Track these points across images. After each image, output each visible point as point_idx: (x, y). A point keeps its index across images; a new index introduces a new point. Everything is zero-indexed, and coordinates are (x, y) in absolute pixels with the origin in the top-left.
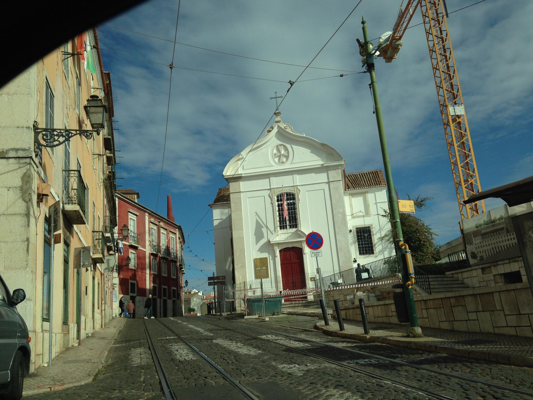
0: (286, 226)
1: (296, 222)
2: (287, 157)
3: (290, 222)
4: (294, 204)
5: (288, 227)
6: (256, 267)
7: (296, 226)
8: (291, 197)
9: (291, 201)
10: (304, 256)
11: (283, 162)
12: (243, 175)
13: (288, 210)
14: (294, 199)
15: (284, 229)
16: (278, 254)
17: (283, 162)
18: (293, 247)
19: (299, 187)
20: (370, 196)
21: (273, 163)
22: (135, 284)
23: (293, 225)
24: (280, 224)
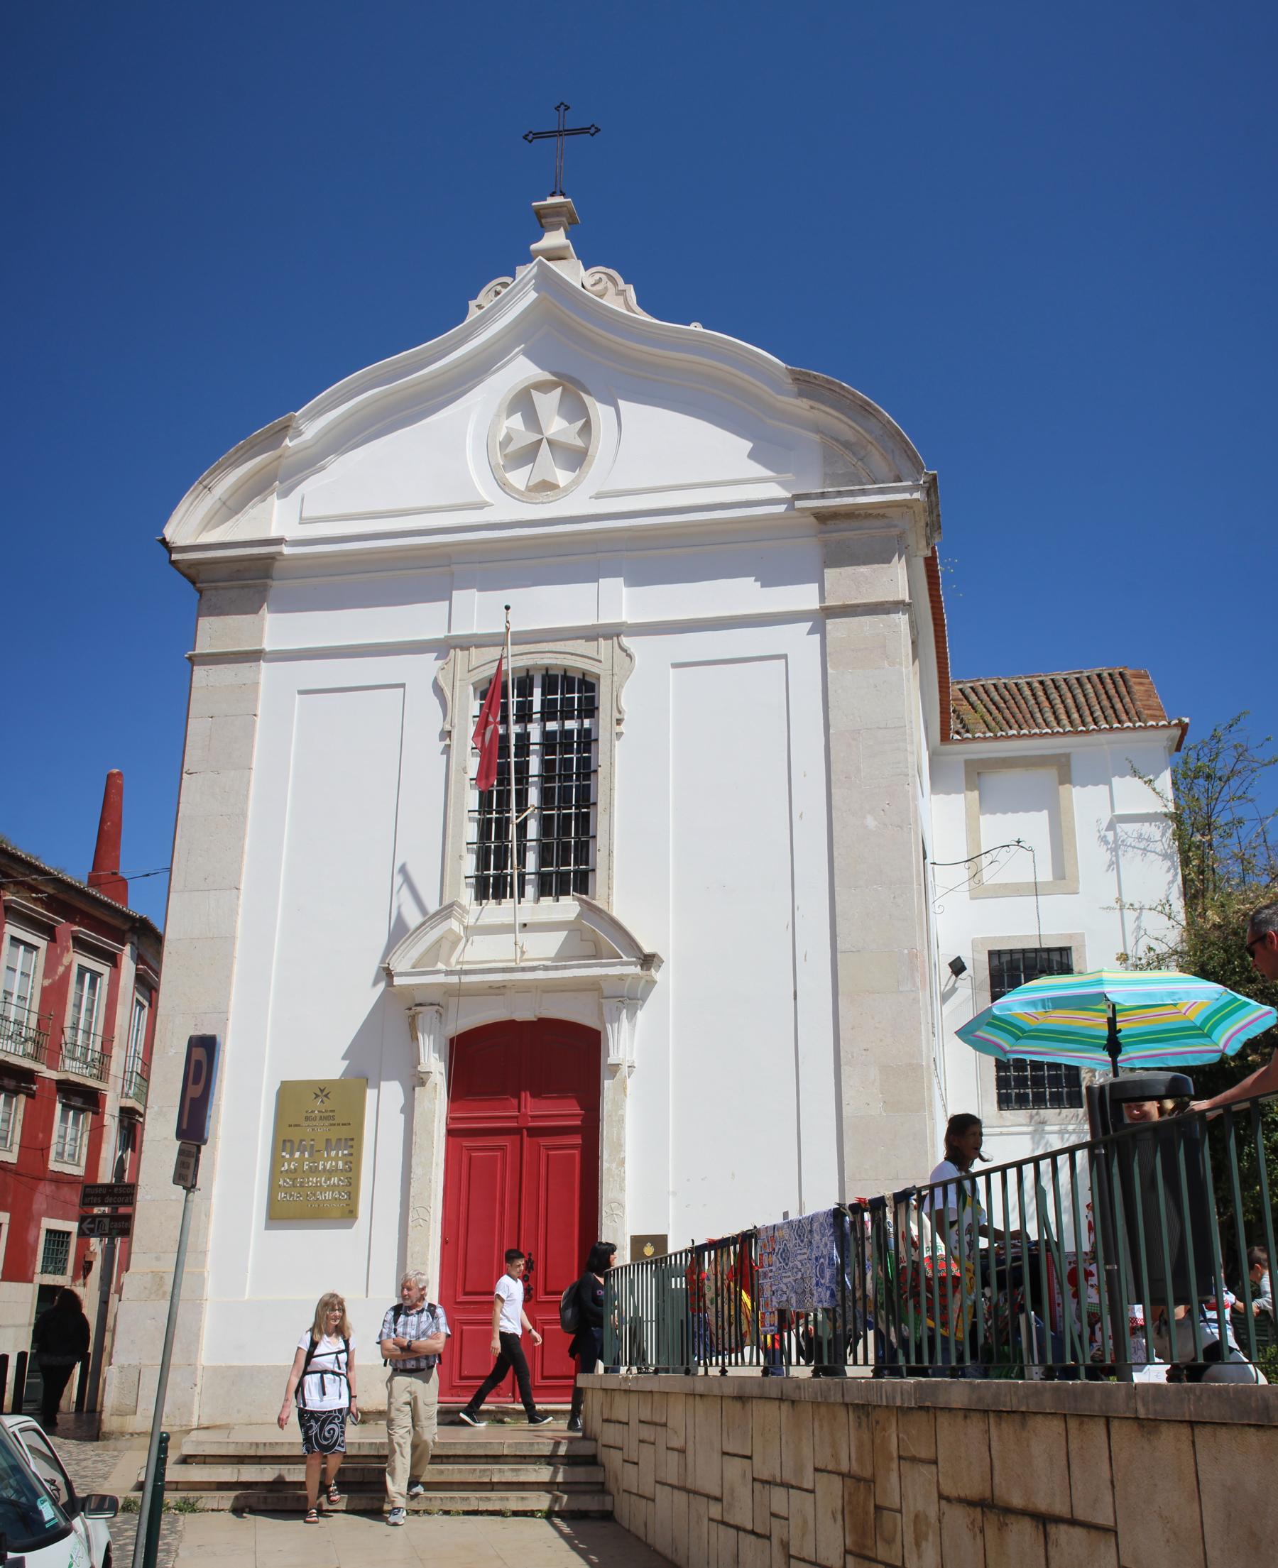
2: (576, 458)
3: (543, 860)
4: (587, 740)
6: (282, 1143)
7: (582, 883)
8: (574, 694)
9: (571, 725)
10: (607, 1085)
11: (547, 486)
12: (286, 550)
13: (540, 781)
14: (589, 709)
15: (499, 895)
16: (434, 1064)
17: (547, 486)
18: (542, 1021)
19: (625, 641)
20: (1087, 804)
21: (484, 488)
24: (483, 863)
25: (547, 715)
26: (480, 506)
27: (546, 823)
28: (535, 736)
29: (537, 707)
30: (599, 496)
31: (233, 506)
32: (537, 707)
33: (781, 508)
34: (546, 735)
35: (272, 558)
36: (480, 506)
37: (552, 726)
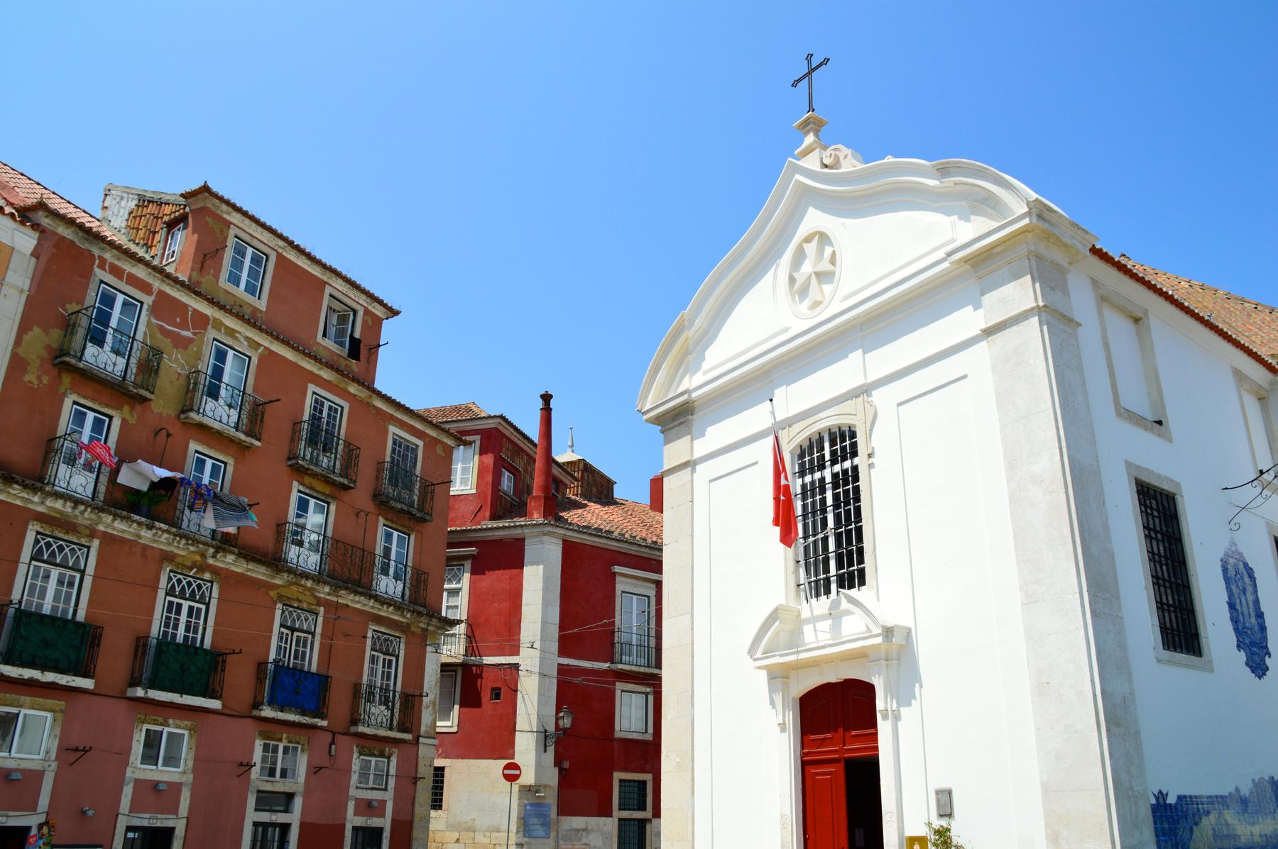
0: (827, 581)
1: (861, 561)
3: (840, 566)
5: (834, 587)
8: (844, 442)
9: (847, 464)
22: (644, 783)
23: (851, 574)
25: (834, 462)
26: (786, 330)
27: (838, 537)
28: (828, 479)
29: (827, 457)
30: (846, 298)
31: (672, 380)
32: (827, 457)
33: (946, 265)
34: (835, 476)
35: (686, 403)
36: (786, 330)
37: (837, 468)
